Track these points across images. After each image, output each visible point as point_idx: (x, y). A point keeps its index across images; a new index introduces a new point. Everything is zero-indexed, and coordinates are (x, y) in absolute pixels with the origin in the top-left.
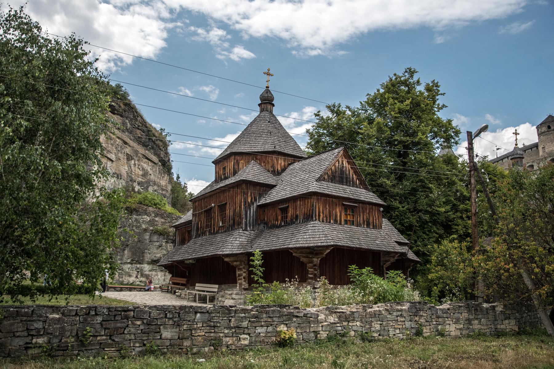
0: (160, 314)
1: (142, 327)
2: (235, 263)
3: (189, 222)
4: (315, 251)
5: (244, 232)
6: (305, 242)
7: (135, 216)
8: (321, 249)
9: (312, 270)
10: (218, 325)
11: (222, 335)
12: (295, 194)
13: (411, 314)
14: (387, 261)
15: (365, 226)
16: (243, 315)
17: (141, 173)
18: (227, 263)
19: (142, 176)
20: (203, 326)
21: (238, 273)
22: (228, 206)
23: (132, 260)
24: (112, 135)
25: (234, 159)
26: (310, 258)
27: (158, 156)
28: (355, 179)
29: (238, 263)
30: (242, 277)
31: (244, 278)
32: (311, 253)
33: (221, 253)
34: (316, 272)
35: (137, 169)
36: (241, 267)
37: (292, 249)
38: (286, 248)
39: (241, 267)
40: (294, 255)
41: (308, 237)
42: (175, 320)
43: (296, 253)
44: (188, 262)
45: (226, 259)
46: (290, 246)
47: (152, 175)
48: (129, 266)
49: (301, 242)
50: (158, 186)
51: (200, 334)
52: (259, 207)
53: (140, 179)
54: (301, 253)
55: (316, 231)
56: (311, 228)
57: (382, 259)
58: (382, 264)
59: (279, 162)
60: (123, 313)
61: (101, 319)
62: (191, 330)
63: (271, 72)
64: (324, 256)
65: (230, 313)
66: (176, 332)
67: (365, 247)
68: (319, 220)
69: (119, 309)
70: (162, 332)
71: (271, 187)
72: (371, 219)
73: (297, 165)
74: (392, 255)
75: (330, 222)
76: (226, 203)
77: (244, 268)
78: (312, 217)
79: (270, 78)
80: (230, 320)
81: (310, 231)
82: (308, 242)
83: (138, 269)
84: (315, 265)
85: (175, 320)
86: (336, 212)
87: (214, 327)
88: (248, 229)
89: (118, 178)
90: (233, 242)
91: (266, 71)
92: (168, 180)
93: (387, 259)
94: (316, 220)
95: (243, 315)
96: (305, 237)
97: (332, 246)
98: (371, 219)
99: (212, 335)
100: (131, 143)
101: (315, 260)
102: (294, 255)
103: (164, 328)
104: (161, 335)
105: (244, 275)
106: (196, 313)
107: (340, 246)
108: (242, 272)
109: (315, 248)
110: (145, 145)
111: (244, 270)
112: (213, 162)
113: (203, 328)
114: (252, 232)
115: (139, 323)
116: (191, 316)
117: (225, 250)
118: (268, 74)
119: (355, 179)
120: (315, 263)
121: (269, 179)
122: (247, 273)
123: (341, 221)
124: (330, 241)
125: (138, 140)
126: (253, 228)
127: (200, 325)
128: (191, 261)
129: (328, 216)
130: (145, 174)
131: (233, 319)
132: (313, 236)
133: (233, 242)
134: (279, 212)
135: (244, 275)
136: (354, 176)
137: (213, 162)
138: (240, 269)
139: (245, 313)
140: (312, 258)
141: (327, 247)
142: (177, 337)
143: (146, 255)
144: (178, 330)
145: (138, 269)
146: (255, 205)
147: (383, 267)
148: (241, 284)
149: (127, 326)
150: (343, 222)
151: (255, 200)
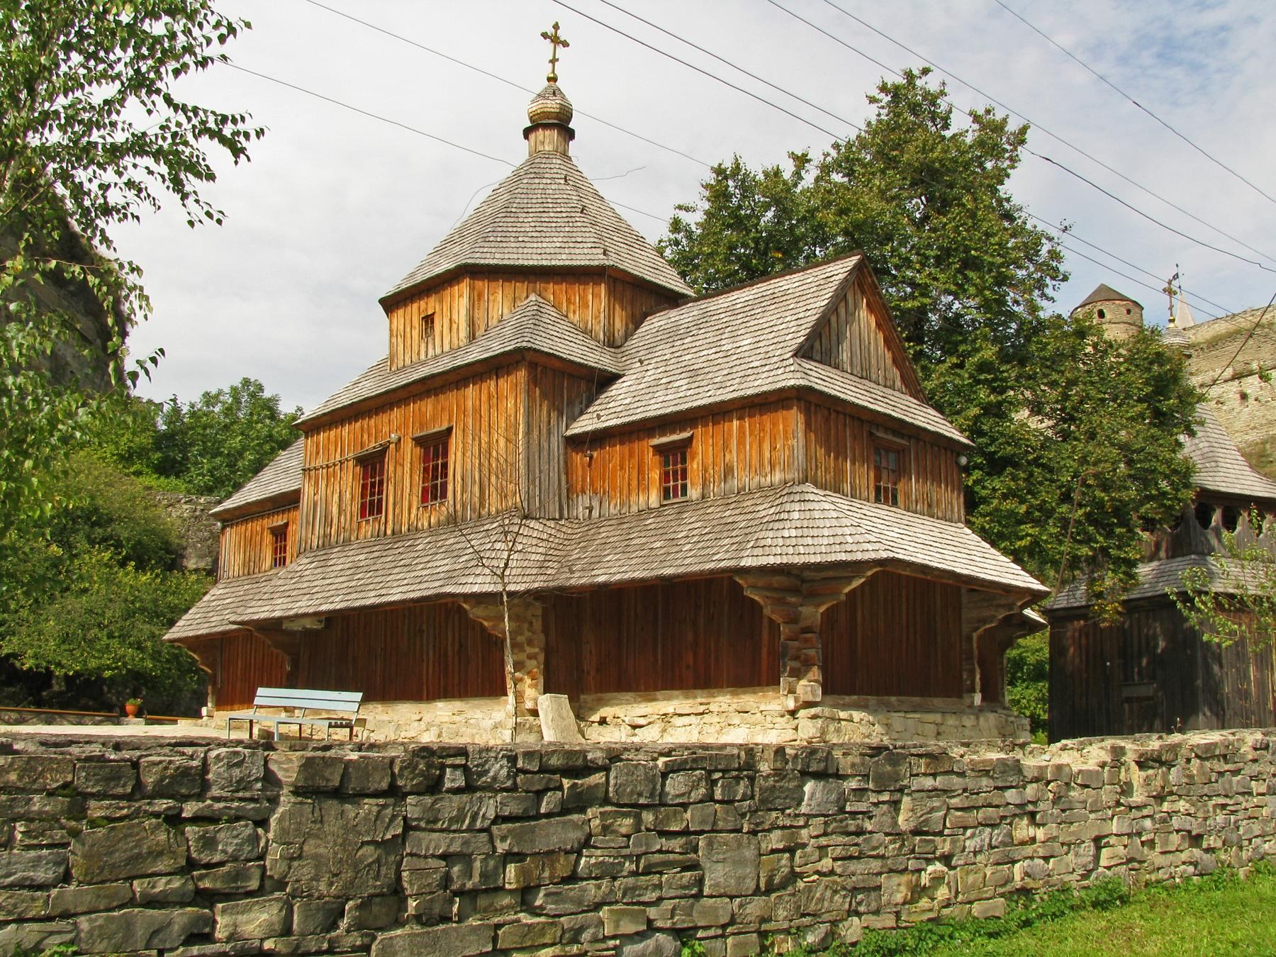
0: (695, 787)
4: (803, 581)
6: (791, 550)
8: (831, 574)
9: (796, 643)
16: (929, 783)
20: (825, 834)
22: (455, 443)
25: (472, 289)
32: (795, 591)
38: (724, 570)
40: (748, 593)
41: (793, 533)
43: (754, 587)
44: (296, 626)
51: (819, 866)
54: (769, 588)
55: (817, 514)
56: (797, 506)
57: (967, 614)
58: (965, 629)
61: (491, 814)
62: (791, 850)
63: (562, 35)
71: (606, 380)
76: (450, 430)
77: (530, 643)
79: (560, 49)
80: (895, 804)
81: (796, 515)
91: (551, 31)
93: (986, 613)
95: (929, 783)
101: (806, 610)
104: (700, 882)
109: (807, 574)
111: (529, 650)
118: (556, 40)
121: (600, 359)
122: (541, 657)
124: (877, 546)
127: (817, 825)
128: (309, 624)
134: (650, 458)
139: (934, 775)
141: (856, 567)
147: (970, 638)
148: (519, 697)
149: (586, 843)
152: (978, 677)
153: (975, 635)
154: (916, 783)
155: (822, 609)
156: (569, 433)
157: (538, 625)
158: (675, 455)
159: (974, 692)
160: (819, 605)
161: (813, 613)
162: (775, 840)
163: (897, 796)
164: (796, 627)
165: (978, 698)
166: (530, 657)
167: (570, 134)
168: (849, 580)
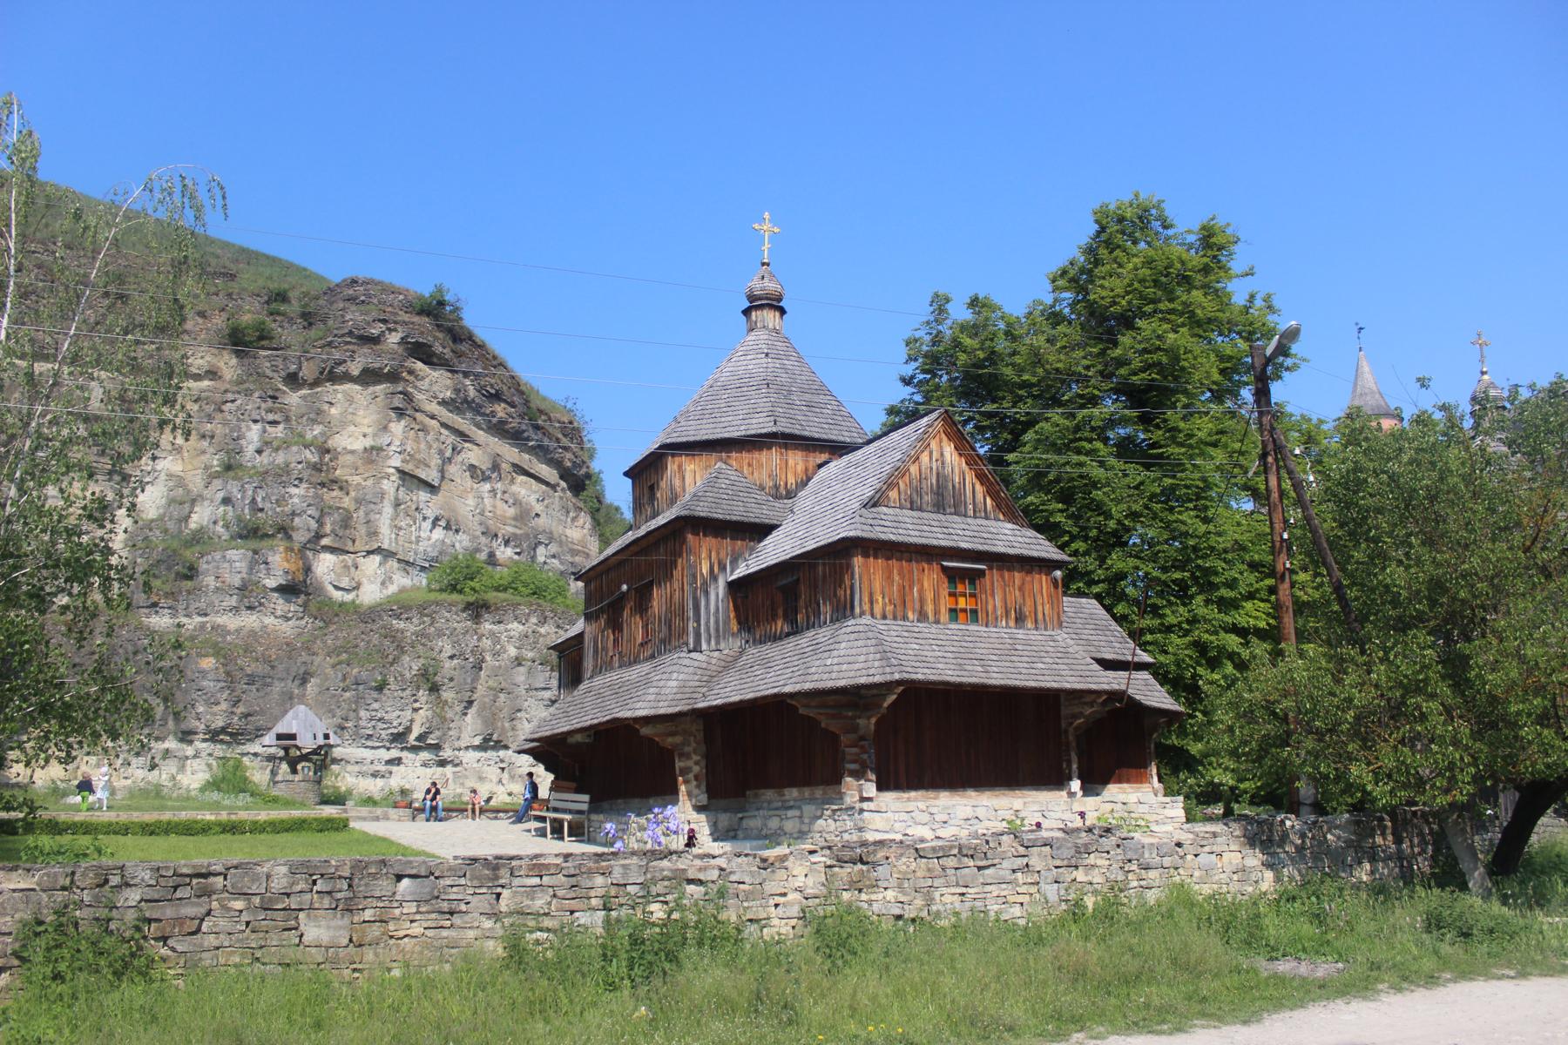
1: (245, 917)
2: (670, 740)
3: (581, 636)
5: (693, 655)
7: (488, 626)
9: (854, 750)
10: (463, 907)
11: (471, 934)
12: (811, 546)
13: (1058, 863)
14: (1075, 717)
15: (1012, 623)
16: (536, 881)
17: (511, 512)
18: (650, 740)
19: (515, 519)
20: (418, 912)
21: (679, 764)
23: (486, 740)
24: (427, 420)
26: (846, 717)
27: (556, 464)
28: (980, 496)
29: (678, 739)
30: (691, 776)
31: (696, 778)
33: (628, 714)
34: (865, 756)
35: (500, 504)
36: (686, 749)
37: (792, 695)
39: (686, 749)
40: (801, 711)
42: (339, 895)
44: (571, 740)
45: (645, 731)
46: (787, 689)
47: (543, 515)
48: (478, 754)
49: (816, 677)
50: (561, 544)
52: (733, 586)
53: (510, 529)
56: (846, 637)
57: (1064, 711)
59: (791, 462)
60: (195, 881)
61: (138, 898)
64: (883, 711)
65: (497, 878)
66: (341, 928)
67: (996, 679)
68: (872, 615)
69: (185, 871)
70: (302, 927)
71: (761, 531)
72: (1029, 602)
73: (836, 466)
74: (1088, 699)
75: (905, 618)
77: (695, 751)
78: (852, 607)
80: (499, 895)
82: (834, 675)
83: (502, 761)
84: (862, 738)
85: (339, 895)
86: (921, 591)
87: (452, 913)
88: (704, 646)
89: (448, 527)
90: (662, 683)
92: (588, 526)
93: (1076, 710)
94: (862, 614)
95: (536, 881)
96: (829, 662)
97: (899, 683)
98: (1029, 602)
99: (445, 933)
100: (480, 435)
101: (862, 722)
102: (801, 711)
103: (308, 916)
105: (696, 769)
106: (399, 878)
107: (919, 682)
108: (690, 763)
110: (516, 437)
111: (696, 758)
112: (626, 474)
113: (418, 917)
114: (716, 654)
115: (239, 904)
116: (383, 886)
117: (639, 705)
119: (980, 496)
120: (861, 732)
122: (703, 763)
123: (937, 612)
125: (499, 429)
126: (718, 643)
129: (898, 602)
130: (524, 515)
131: (506, 893)
132: (851, 659)
133: (662, 683)
135: (696, 769)
136: (978, 487)
137: (626, 474)
138: (683, 755)
140: (854, 718)
141: (888, 686)
142: (346, 941)
143: (519, 726)
144: (346, 921)
145: (502, 761)
146: (721, 583)
147: (1066, 732)
149: (209, 913)
150: (944, 616)
151: (723, 568)
152: (1075, 766)
153: (1071, 730)
154: (516, 882)
155: (873, 720)
156: (734, 577)
157: (700, 736)
158: (791, 594)
159: (1070, 779)
160: (869, 718)
161: (869, 724)
162: (368, 915)
163: (499, 890)
164: (853, 736)
165: (1076, 785)
166: (697, 763)
167: (782, 311)
168: (884, 697)
